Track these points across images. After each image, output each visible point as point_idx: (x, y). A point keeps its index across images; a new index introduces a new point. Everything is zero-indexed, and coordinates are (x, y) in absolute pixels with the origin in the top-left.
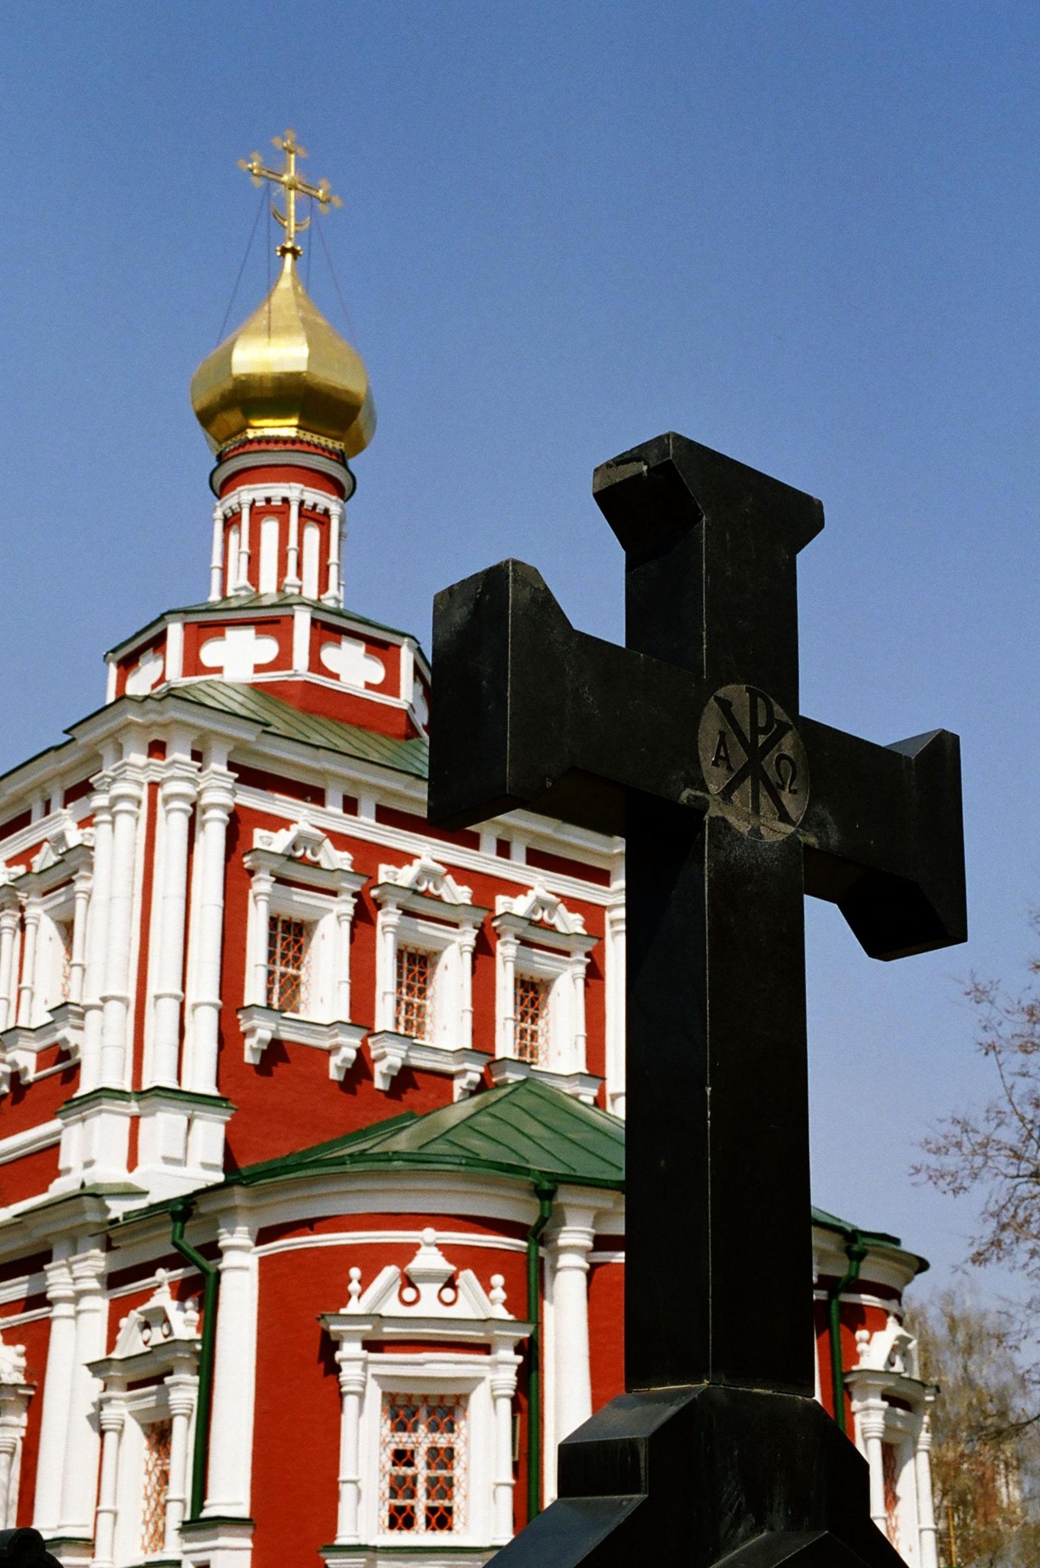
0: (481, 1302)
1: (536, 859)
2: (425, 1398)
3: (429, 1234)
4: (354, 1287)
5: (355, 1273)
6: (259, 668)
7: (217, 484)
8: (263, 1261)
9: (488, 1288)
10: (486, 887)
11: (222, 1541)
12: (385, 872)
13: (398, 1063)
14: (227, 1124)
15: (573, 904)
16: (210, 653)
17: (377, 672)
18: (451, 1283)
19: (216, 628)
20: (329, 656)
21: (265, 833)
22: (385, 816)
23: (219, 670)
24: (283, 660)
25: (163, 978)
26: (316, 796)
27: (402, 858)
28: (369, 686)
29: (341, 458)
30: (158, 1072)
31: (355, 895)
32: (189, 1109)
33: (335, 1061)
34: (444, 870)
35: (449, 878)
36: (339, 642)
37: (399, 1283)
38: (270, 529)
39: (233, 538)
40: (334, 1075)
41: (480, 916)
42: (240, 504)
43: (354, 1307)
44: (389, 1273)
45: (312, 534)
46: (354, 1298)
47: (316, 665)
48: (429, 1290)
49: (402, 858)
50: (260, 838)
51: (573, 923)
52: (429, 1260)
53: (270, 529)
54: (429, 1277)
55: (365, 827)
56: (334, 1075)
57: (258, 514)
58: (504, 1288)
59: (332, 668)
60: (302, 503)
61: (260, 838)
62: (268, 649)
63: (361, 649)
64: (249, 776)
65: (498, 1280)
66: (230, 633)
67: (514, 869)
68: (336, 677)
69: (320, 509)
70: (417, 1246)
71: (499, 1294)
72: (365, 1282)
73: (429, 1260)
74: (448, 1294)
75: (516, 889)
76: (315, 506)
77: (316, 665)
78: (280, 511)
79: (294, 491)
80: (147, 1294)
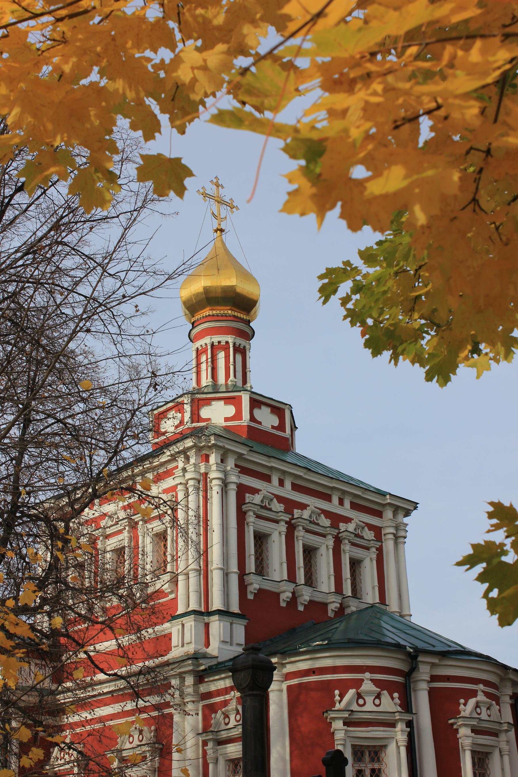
0: (389, 704)
1: (354, 506)
2: (368, 746)
3: (367, 675)
4: (337, 698)
5: (337, 692)
6: (226, 419)
8: (289, 688)
9: (393, 698)
10: (336, 519)
12: (297, 513)
13: (308, 599)
14: (246, 627)
15: (371, 527)
16: (205, 412)
17: (275, 421)
18: (378, 696)
19: (208, 402)
20: (257, 413)
21: (251, 495)
22: (295, 487)
23: (209, 419)
24: (238, 416)
26: (267, 479)
27: (303, 506)
28: (273, 427)
29: (248, 323)
31: (286, 522)
32: (230, 619)
34: (320, 512)
35: (322, 516)
36: (260, 408)
37: (356, 696)
40: (283, 604)
41: (335, 532)
42: (206, 344)
43: (338, 706)
44: (351, 692)
45: (239, 357)
46: (337, 704)
48: (369, 699)
49: (303, 506)
50: (248, 497)
51: (369, 535)
52: (367, 686)
54: (369, 693)
56: (283, 604)
58: (399, 698)
59: (259, 419)
60: (234, 344)
61: (248, 497)
62: (231, 411)
63: (269, 410)
64: (244, 471)
65: (396, 695)
67: (346, 511)
68: (260, 423)
69: (242, 347)
70: (362, 680)
71: (398, 701)
72: (342, 696)
73: (367, 686)
74: (377, 702)
75: (348, 520)
76: (240, 345)
77: (252, 418)
78: (226, 348)
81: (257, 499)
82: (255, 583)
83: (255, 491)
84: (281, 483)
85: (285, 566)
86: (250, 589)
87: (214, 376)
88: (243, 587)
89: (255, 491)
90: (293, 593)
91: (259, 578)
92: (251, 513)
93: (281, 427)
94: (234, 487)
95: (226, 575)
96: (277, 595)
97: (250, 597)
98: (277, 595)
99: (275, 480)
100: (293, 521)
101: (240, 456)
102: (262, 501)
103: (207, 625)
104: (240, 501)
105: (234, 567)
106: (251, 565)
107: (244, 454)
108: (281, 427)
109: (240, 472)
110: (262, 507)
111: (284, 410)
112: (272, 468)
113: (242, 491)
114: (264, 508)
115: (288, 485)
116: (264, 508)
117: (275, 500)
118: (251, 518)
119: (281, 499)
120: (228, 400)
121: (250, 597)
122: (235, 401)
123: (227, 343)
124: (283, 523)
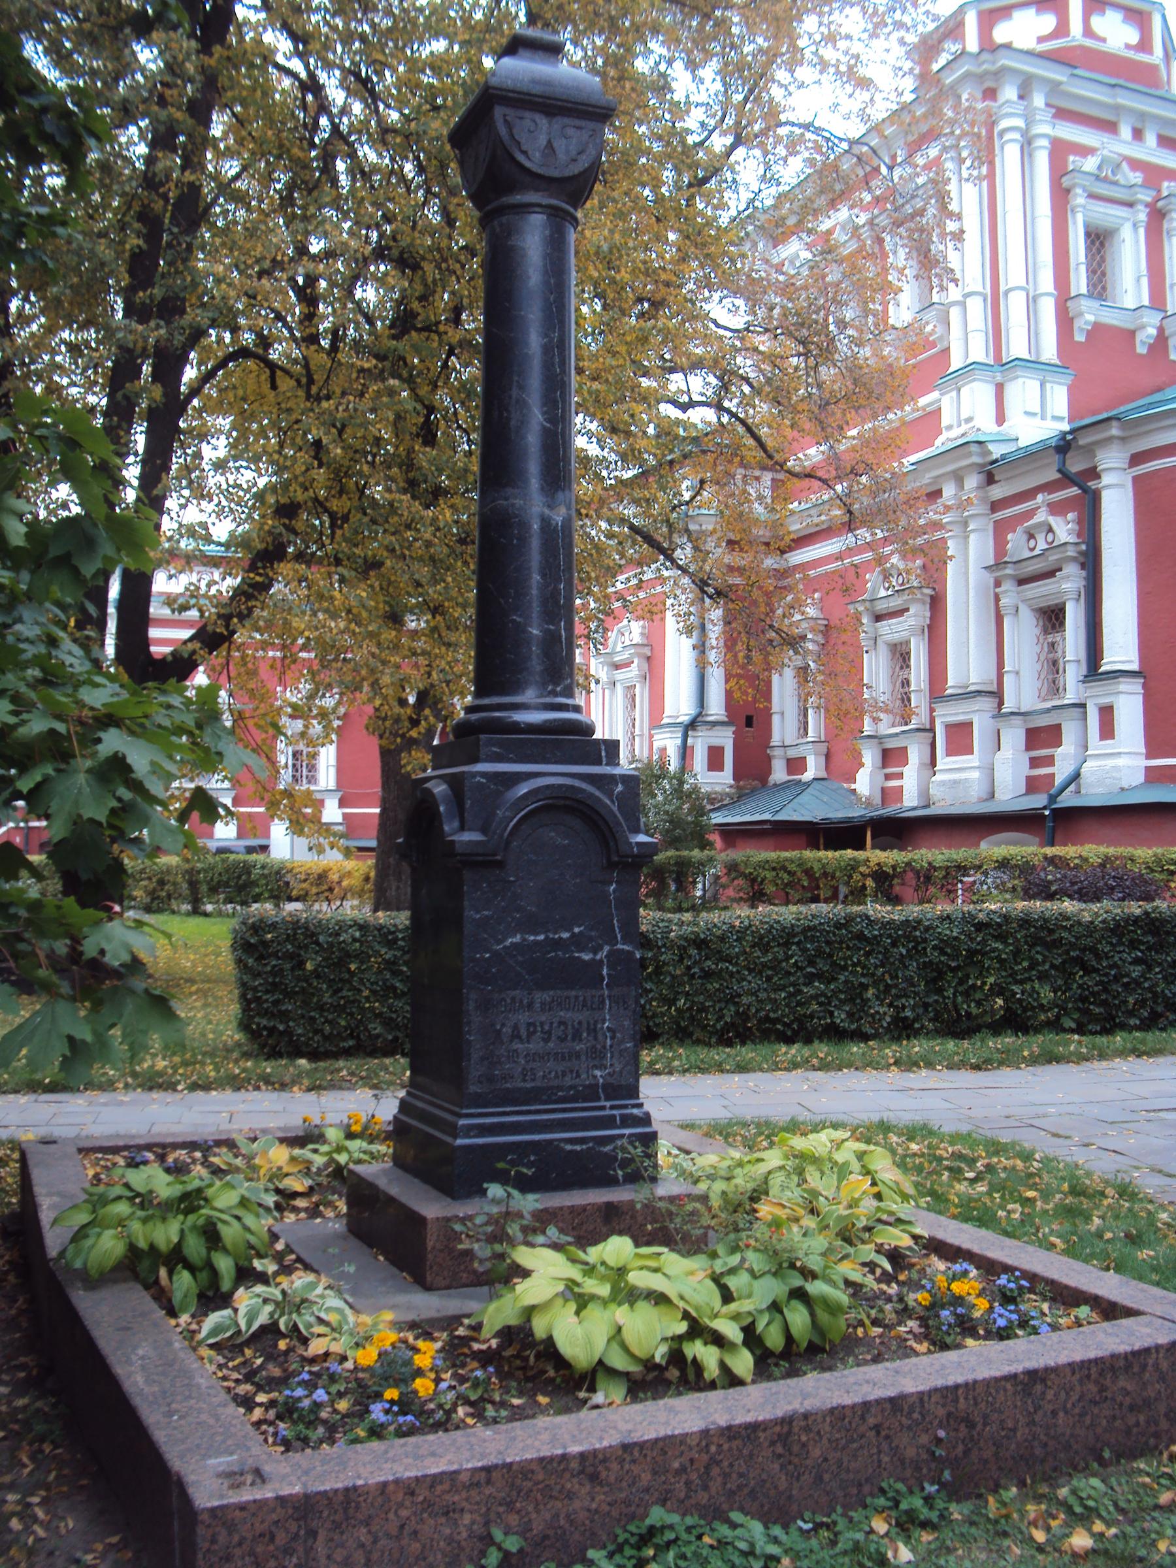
6: (1041, 40)
8: (1136, 480)
11: (1122, 687)
17: (1132, 35)
22: (1165, 142)
24: (1062, 29)
25: (1013, 273)
26: (1110, 127)
28: (1128, 46)
30: (1017, 347)
33: (1140, 337)
40: (1141, 350)
47: (1088, 32)
55: (1150, 151)
56: (1141, 350)
64: (1062, 114)
68: (1104, 40)
77: (1088, 32)
80: (1031, 513)
81: (1090, 164)
82: (1089, 314)
83: (1085, 151)
84: (1138, 134)
85: (1145, 282)
86: (1078, 324)
88: (1065, 321)
89: (1085, 151)
90: (1161, 330)
91: (1095, 304)
92: (1079, 191)
93: (1144, 45)
94: (1045, 143)
95: (1032, 302)
96: (1130, 335)
97: (1080, 337)
98: (1130, 335)
99: (1126, 132)
100: (1160, 204)
101: (1054, 88)
102: (1099, 168)
103: (1000, 389)
104: (1058, 171)
105: (1046, 281)
106: (1080, 282)
107: (1060, 83)
108: (1144, 45)
109: (1055, 116)
110: (1097, 178)
111: (1149, 14)
112: (1118, 108)
113: (1060, 150)
114: (1105, 180)
115: (1151, 139)
116: (1105, 180)
117: (1125, 165)
118: (1079, 199)
119: (1135, 165)
121: (1080, 337)
124: (1140, 207)
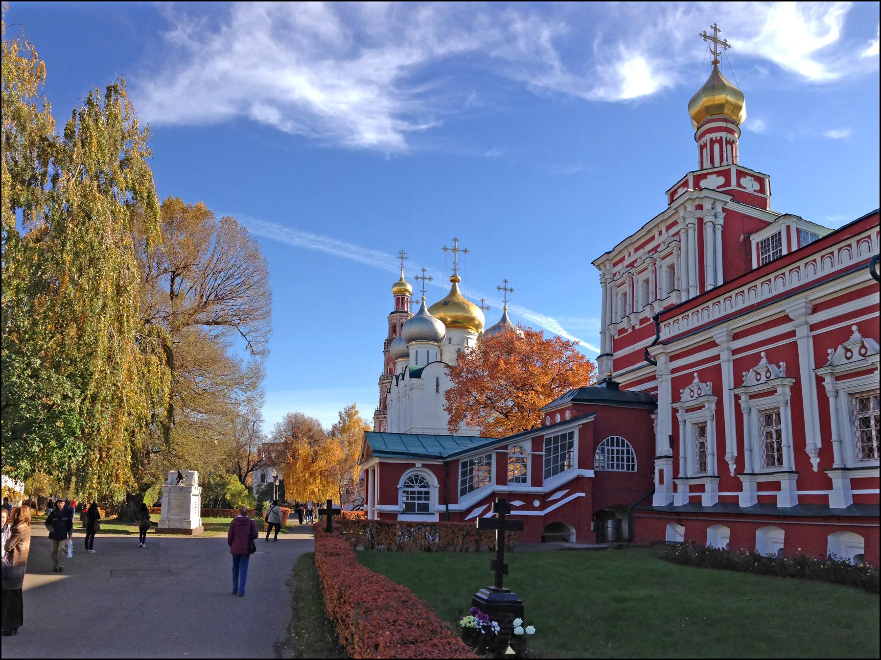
6: (719, 187)
7: (697, 137)
16: (703, 184)
17: (757, 186)
19: (704, 176)
24: (728, 183)
38: (717, 147)
39: (705, 151)
47: (739, 185)
53: (717, 147)
57: (712, 142)
62: (722, 180)
66: (709, 177)
77: (739, 185)
78: (720, 141)
79: (724, 135)
87: (712, 162)
120: (719, 174)
122: (726, 174)
123: (721, 138)
